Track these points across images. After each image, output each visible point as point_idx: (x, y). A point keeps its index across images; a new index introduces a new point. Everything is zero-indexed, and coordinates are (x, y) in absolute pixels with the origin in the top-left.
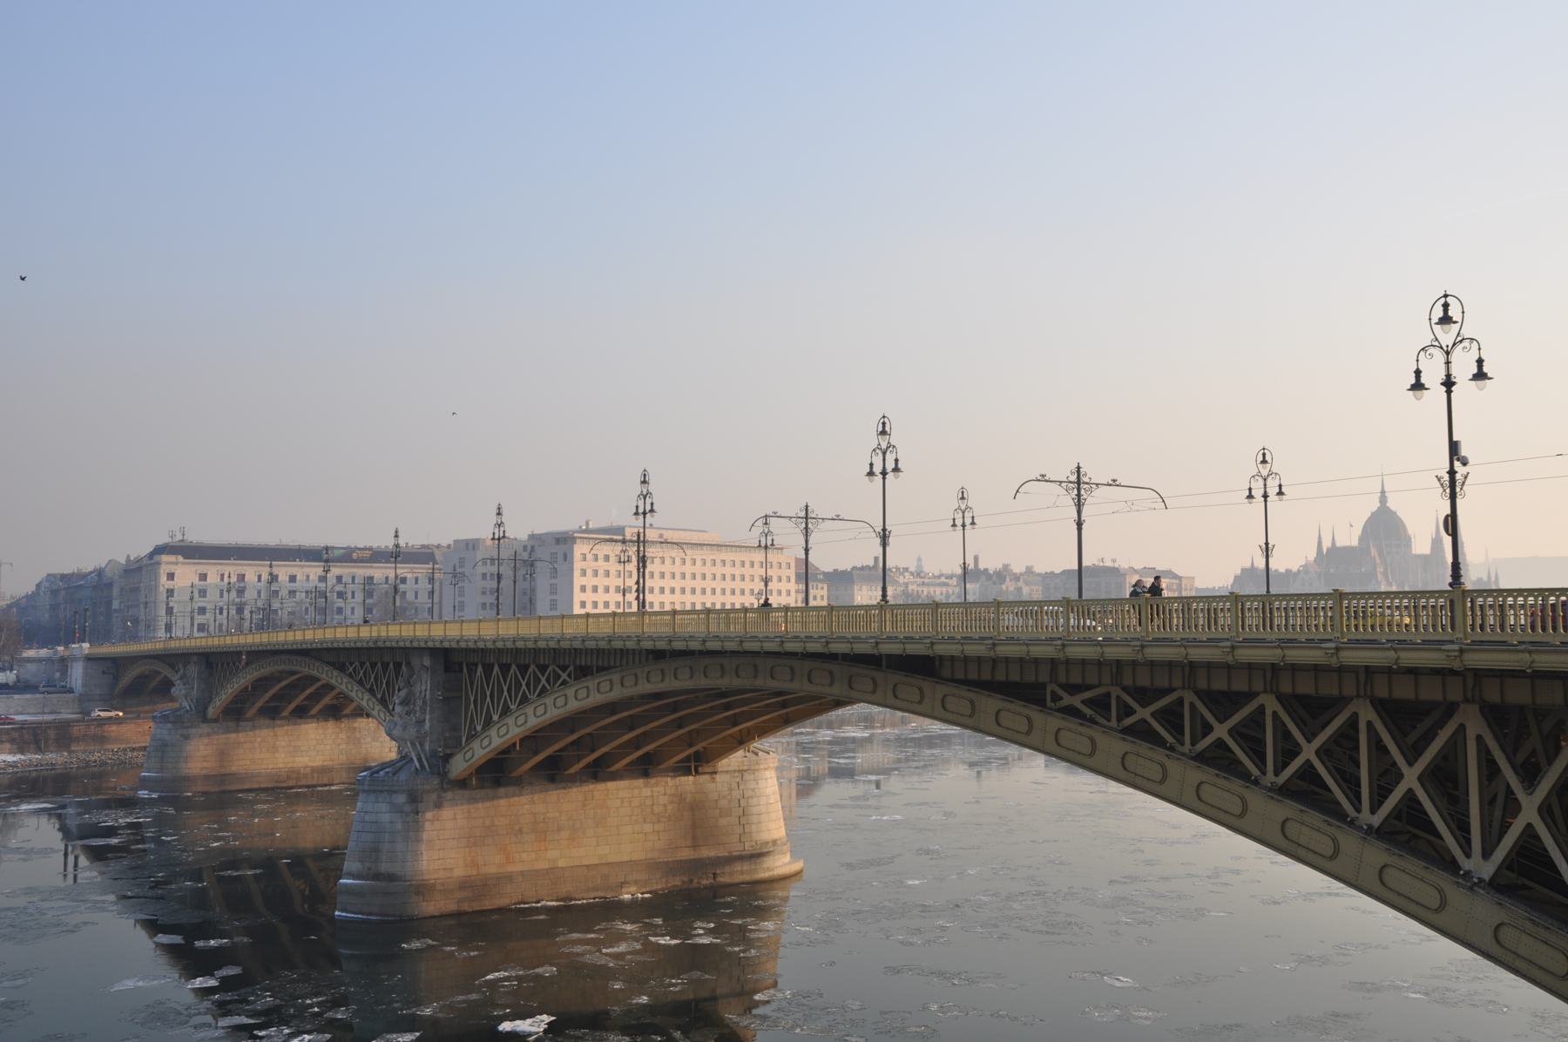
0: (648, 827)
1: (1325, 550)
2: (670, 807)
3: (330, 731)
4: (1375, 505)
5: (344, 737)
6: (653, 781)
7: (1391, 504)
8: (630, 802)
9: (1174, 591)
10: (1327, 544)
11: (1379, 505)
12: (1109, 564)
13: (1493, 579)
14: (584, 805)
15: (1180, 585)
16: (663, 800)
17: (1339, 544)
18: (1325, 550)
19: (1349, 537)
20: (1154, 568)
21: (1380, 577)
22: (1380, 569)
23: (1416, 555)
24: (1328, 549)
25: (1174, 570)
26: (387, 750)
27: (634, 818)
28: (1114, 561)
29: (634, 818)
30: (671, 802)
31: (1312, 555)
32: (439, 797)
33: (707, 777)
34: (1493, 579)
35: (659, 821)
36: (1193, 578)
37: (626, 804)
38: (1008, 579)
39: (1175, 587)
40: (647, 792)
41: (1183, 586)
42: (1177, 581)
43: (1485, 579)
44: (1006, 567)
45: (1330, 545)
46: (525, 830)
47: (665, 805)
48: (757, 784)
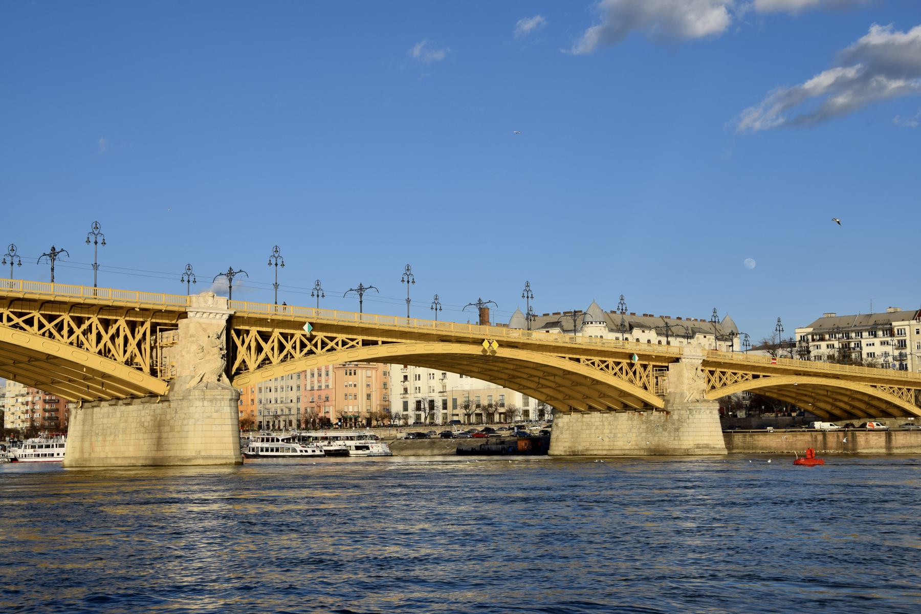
0: (141, 436)
2: (150, 424)
3: (635, 423)
5: (645, 427)
6: (146, 405)
8: (137, 419)
14: (120, 420)
16: (149, 418)
26: (672, 438)
27: (137, 429)
29: (137, 429)
30: (152, 420)
32: (76, 413)
33: (166, 404)
35: (146, 433)
37: (135, 421)
40: (143, 413)
46: (100, 434)
47: (149, 422)
48: (189, 410)
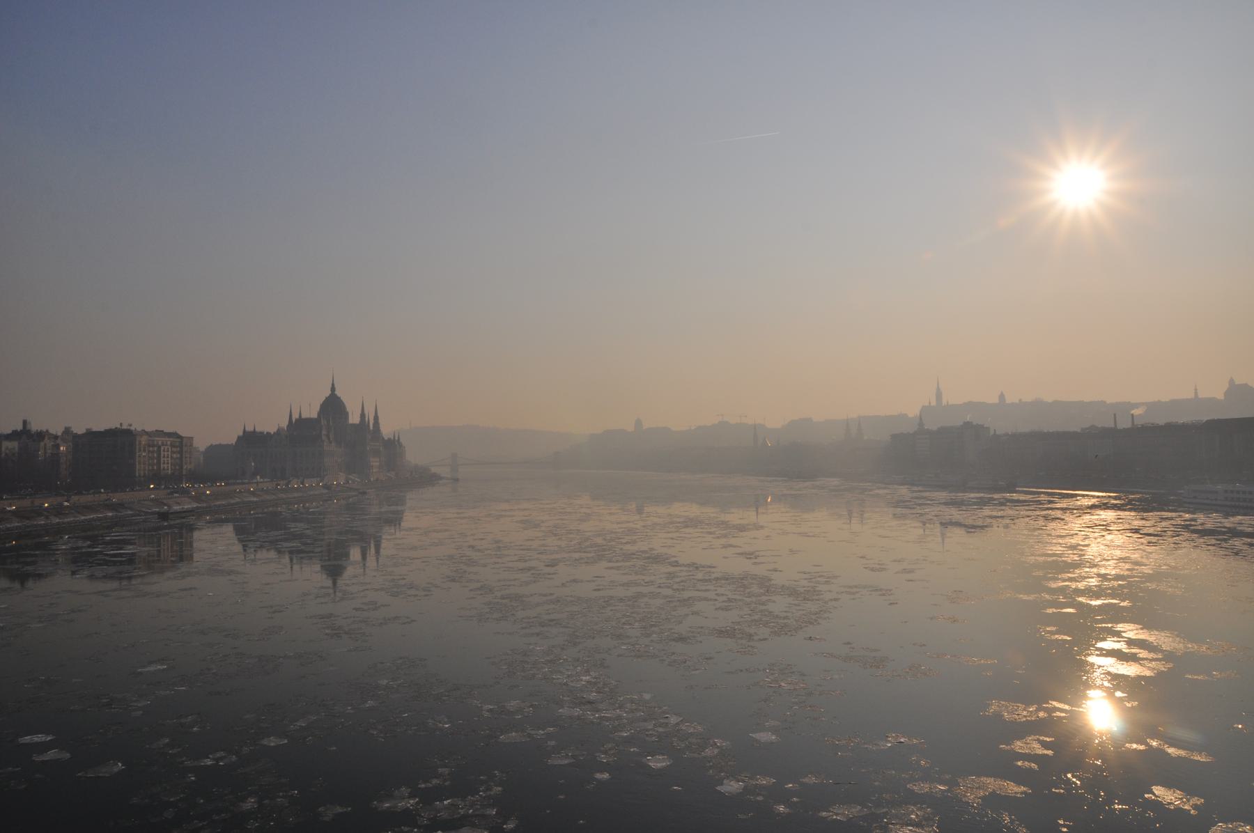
1: (294, 421)
4: (328, 393)
7: (338, 393)
9: (177, 447)
10: (295, 416)
11: (330, 392)
12: (125, 427)
13: (396, 438)
15: (181, 442)
17: (304, 416)
18: (294, 421)
19: (312, 412)
20: (162, 431)
21: (324, 438)
22: (324, 432)
23: (352, 425)
24: (296, 420)
25: (179, 432)
28: (130, 425)
31: (284, 424)
34: (396, 438)
36: (192, 438)
38: (46, 438)
39: (178, 444)
41: (184, 444)
42: (179, 440)
43: (392, 438)
44: (47, 431)
45: (297, 417)
